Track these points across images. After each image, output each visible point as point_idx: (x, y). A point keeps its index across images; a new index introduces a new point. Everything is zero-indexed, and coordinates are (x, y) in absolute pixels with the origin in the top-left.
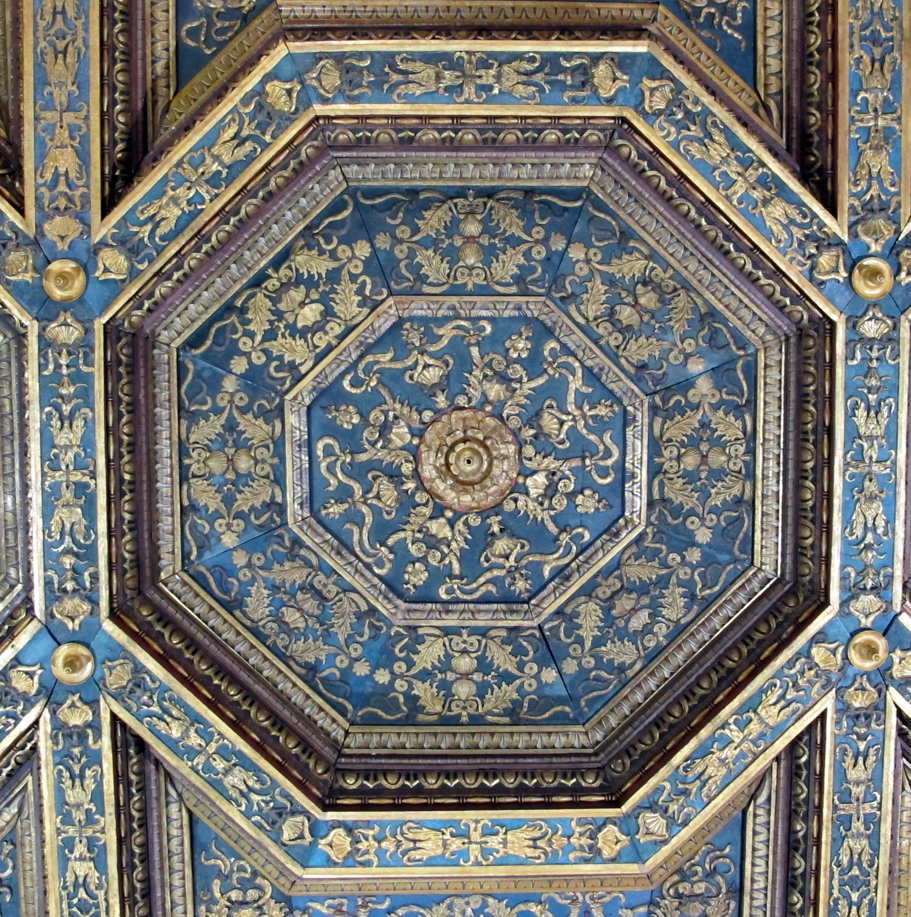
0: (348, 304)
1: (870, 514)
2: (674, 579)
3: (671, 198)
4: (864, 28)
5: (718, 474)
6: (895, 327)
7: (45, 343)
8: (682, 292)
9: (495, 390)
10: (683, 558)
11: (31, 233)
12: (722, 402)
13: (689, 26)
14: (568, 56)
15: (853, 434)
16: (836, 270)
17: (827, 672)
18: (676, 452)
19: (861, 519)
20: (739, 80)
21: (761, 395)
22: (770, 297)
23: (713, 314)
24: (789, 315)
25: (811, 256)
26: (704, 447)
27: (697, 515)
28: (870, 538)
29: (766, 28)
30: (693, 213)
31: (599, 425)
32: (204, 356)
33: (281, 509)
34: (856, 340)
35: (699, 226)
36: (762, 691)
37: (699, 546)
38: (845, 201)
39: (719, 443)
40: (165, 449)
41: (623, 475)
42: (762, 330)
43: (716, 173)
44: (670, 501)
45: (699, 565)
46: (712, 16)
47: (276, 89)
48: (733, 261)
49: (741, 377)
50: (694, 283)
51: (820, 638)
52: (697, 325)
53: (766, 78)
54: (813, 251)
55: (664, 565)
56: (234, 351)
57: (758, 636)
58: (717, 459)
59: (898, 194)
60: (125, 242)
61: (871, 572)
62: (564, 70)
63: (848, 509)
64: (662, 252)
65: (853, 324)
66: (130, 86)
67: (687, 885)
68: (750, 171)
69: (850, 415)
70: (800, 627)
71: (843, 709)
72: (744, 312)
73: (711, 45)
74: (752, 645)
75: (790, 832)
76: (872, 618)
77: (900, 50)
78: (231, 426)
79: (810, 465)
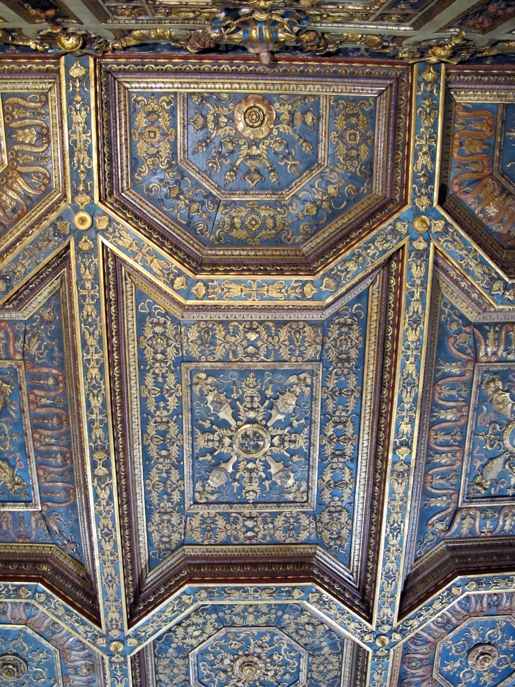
0: (209, 629)
7: (111, 662)
9: (259, 650)
11: (105, 633)
14: (284, 587)
31: (292, 658)
32: (163, 643)
33: (189, 681)
39: (330, 663)
40: (150, 666)
41: (299, 670)
47: (185, 598)
56: (173, 642)
58: (330, 667)
60: (136, 636)
62: (283, 592)
66: (132, 570)
78: (172, 662)
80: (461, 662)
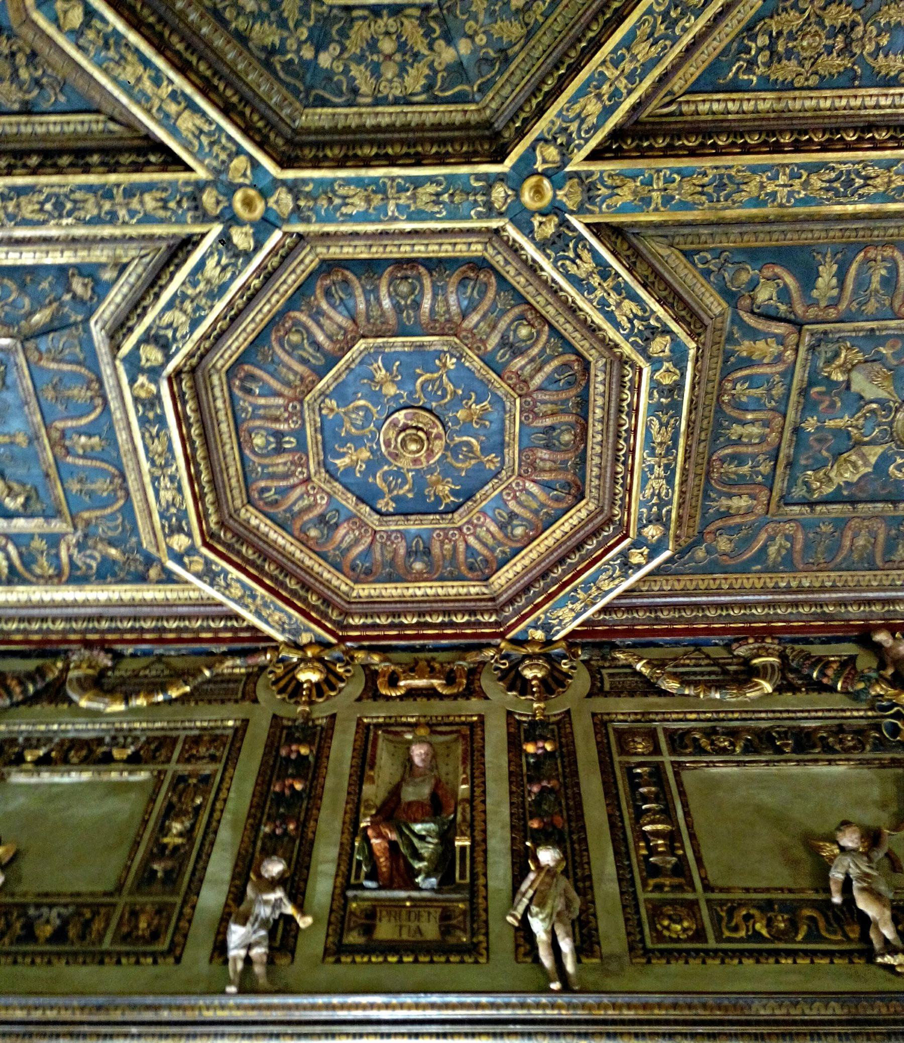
1: (356, 200)
2: (286, 34)
3: (604, 14)
4: (730, 177)
5: (376, 71)
6: (501, 215)
8: (524, 31)
10: (305, 42)
12: (436, 72)
13: (741, 32)
15: (418, 182)
16: (545, 161)
17: (227, 170)
18: (393, 30)
19: (351, 193)
20: (694, 78)
21: (442, 108)
22: (521, 109)
23: (507, 61)
24: (507, 126)
25: (555, 139)
26: (398, 57)
27: (341, 53)
28: (337, 201)
29: (734, 100)
30: (591, 34)
34: (490, 181)
35: (580, 41)
36: (204, 114)
37: (316, 57)
38: (596, 167)
42: (494, 105)
43: (624, 51)
44: (351, 28)
45: (301, 58)
46: (749, 52)
48: (550, 74)
49: (456, 90)
50: (532, 43)
51: (255, 164)
52: (498, 47)
53: (695, 102)
54: (559, 141)
55: (298, 24)
57: (248, 111)
59: (601, 212)
61: (311, 204)
63: (359, 182)
64: (558, 10)
65: (501, 178)
67: (24, 61)
68: (624, 81)
69: (431, 180)
70: (261, 145)
71: (200, 187)
72: (508, 88)
73: (724, 52)
74: (240, 107)
75: (91, 151)
76: (275, 207)
77: (710, 208)
79: (390, 151)
80: (397, 397)
